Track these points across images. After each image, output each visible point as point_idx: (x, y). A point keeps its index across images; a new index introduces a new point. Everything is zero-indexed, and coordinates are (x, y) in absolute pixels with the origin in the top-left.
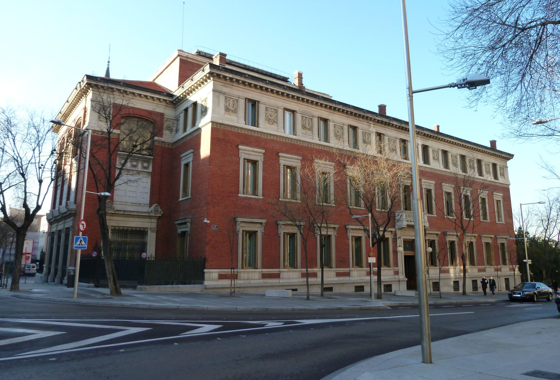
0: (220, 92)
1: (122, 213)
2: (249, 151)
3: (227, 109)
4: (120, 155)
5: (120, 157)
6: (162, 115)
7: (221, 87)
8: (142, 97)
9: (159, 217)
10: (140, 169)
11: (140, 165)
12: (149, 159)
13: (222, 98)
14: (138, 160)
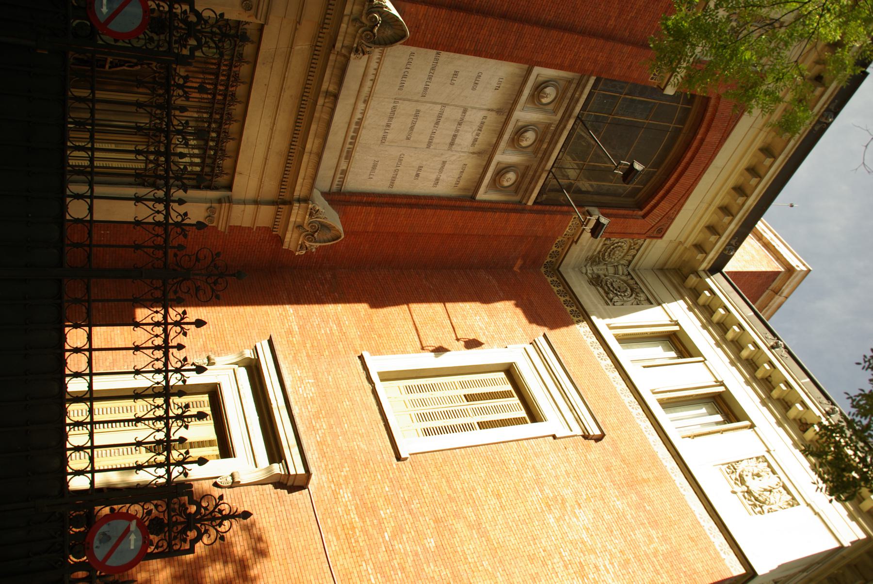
5: (570, 82)
6: (660, 233)
9: (280, 240)
12: (528, 191)
14: (535, 152)
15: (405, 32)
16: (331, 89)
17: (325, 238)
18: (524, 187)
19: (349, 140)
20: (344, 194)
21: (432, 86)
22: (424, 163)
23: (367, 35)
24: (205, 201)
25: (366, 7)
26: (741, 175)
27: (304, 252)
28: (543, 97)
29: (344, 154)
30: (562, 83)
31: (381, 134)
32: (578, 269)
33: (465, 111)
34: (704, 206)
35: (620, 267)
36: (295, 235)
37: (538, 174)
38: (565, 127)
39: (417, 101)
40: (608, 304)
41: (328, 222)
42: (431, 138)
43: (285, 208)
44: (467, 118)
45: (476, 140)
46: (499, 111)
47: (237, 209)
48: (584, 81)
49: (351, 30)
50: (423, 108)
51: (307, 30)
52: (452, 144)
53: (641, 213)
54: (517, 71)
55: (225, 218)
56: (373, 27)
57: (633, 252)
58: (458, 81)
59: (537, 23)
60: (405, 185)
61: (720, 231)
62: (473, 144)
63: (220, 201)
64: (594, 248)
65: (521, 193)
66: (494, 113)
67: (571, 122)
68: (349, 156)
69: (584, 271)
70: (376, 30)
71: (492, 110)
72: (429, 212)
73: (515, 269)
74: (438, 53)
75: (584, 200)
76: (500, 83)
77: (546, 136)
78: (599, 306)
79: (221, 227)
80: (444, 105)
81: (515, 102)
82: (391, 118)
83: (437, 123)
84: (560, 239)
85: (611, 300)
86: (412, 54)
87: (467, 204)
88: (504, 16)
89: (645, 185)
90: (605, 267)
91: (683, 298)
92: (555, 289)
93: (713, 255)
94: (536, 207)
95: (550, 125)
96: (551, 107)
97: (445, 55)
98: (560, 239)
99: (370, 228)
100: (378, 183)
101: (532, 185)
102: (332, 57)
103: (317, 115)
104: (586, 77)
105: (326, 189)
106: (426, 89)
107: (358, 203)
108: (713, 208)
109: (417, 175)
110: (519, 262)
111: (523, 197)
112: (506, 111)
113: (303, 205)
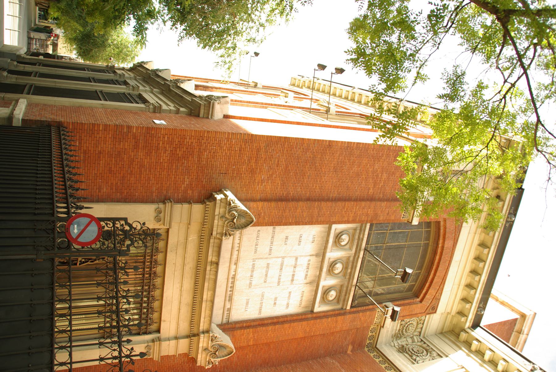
1: (211, 257)
4: (362, 230)
5: (355, 229)
6: (434, 310)
9: (194, 360)
12: (345, 301)
14: (345, 275)
15: (252, 218)
16: (214, 260)
17: (223, 354)
18: (342, 298)
19: (229, 289)
20: (231, 323)
21: (274, 248)
23: (230, 224)
24: (143, 342)
25: (227, 209)
26: (473, 262)
27: (211, 366)
28: (342, 242)
29: (228, 298)
30: (351, 231)
31: (248, 282)
32: (388, 344)
33: (297, 259)
34: (456, 287)
35: (415, 337)
36: (204, 355)
37: (349, 289)
38: (359, 257)
40: (414, 364)
41: (224, 343)
42: (279, 279)
43: (195, 339)
44: (298, 263)
45: (306, 275)
46: (317, 255)
47: (164, 344)
48: (363, 228)
49: (221, 223)
51: (195, 227)
52: (292, 280)
53: (419, 300)
54: (323, 229)
55: (158, 352)
56: (234, 219)
57: (420, 326)
58: (289, 242)
59: (328, 200)
60: (269, 311)
61: (471, 300)
62: (306, 278)
63: (153, 341)
64: (395, 328)
65: (341, 303)
66: (314, 257)
68: (231, 299)
69: (393, 345)
70: (235, 221)
71: (313, 255)
72: (286, 326)
73: (349, 352)
75: (381, 299)
76: (314, 238)
77: (349, 264)
78: (408, 366)
79: (156, 358)
80: (283, 258)
81: (326, 248)
82: (253, 271)
83: (281, 269)
84: (372, 327)
85: (415, 360)
86: (259, 231)
87: (310, 316)
88: (308, 199)
89: (416, 282)
90: (405, 339)
91: (461, 349)
92: (377, 360)
93: (471, 317)
94: (352, 310)
95: (349, 257)
96: (347, 246)
97: (278, 228)
98: (372, 327)
99: (251, 343)
100: (251, 313)
101: (347, 296)
102: (212, 241)
103: (207, 277)
104: (364, 225)
105: (220, 323)
106: (271, 250)
107: (241, 328)
108: (462, 287)
109: (275, 304)
110: (350, 347)
111: (343, 305)
112: (322, 254)
113: (206, 335)
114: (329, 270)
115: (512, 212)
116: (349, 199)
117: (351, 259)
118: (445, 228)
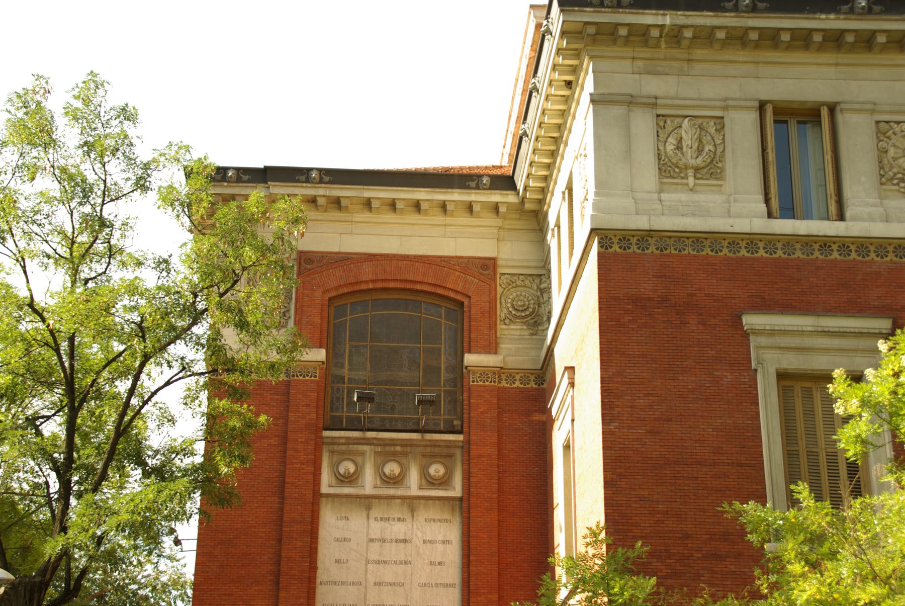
0: (631, 102)
2: (801, 333)
3: (669, 170)
4: (333, 442)
5: (332, 452)
6: (488, 265)
7: (627, 78)
8: (402, 212)
10: (414, 491)
11: (414, 476)
12: (449, 445)
13: (643, 124)
14: (405, 454)
21: (351, 579)
22: (427, 561)
33: (371, 540)
34: (449, 229)
37: (428, 443)
38: (375, 439)
39: (366, 588)
42: (401, 563)
44: (378, 536)
45: (399, 520)
46: (369, 508)
50: (371, 580)
52: (405, 541)
58: (344, 558)
62: (404, 520)
66: (371, 512)
67: (370, 434)
71: (368, 515)
72: (473, 543)
74: (321, 583)
76: (341, 518)
77: (388, 452)
80: (367, 562)
83: (385, 562)
87: (465, 505)
88: (280, 541)
93: (496, 197)
95: (375, 453)
96: (359, 459)
101: (441, 444)
104: (325, 440)
106: (354, 584)
108: (449, 220)
109: (440, 564)
112: (366, 502)
114: (395, 483)
115: (303, 178)
116: (283, 475)
117: (379, 449)
118: (340, 286)
